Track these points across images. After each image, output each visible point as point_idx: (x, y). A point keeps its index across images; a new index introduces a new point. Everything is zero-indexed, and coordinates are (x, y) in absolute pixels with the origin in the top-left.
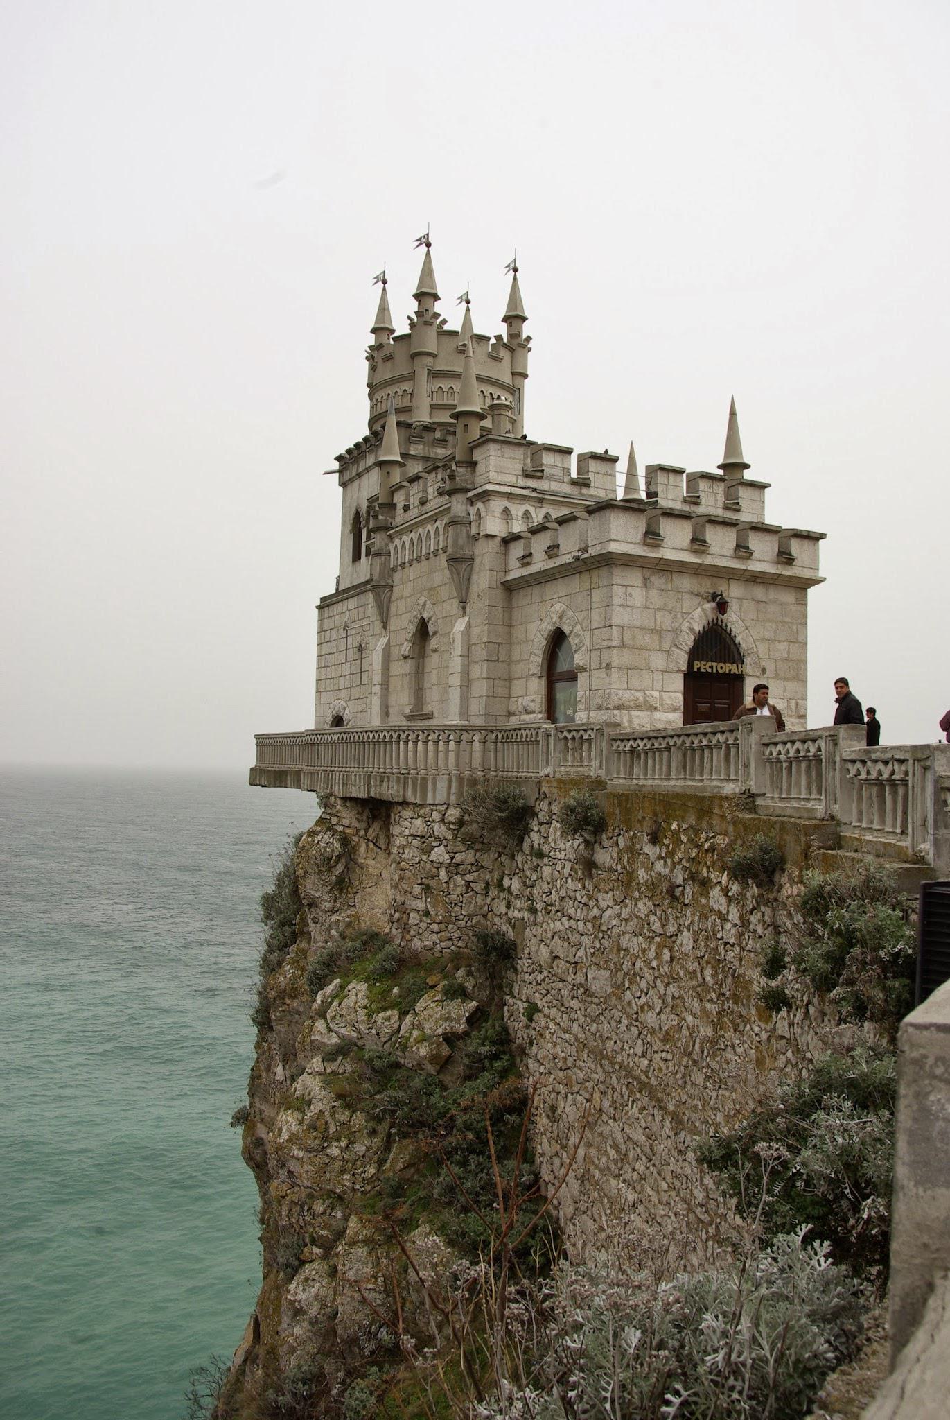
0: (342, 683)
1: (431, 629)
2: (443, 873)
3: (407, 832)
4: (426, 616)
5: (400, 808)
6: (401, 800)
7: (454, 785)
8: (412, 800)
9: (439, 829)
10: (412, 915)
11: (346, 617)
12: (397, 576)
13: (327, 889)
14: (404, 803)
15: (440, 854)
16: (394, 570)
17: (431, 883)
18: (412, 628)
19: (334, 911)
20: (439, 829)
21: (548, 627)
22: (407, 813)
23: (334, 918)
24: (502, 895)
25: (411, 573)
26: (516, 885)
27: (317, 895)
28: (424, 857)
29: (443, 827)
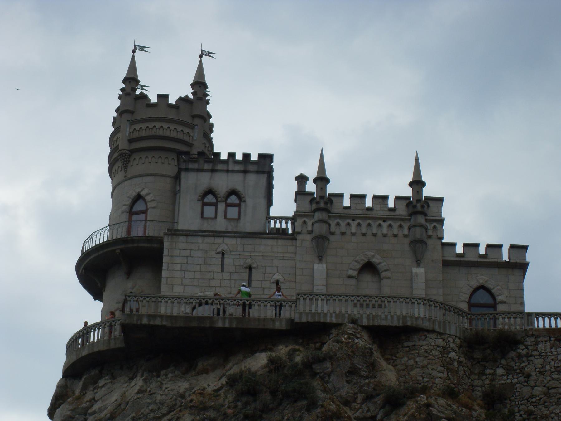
0: (213, 283)
1: (381, 267)
2: (456, 364)
3: (433, 344)
4: (374, 260)
5: (426, 333)
6: (431, 329)
7: (458, 329)
8: (438, 330)
9: (452, 345)
10: (437, 380)
11: (223, 247)
12: (332, 238)
13: (365, 366)
14: (433, 331)
15: (452, 355)
16: (333, 234)
17: (450, 367)
18: (358, 266)
19: (367, 377)
20: (452, 345)
21: (475, 283)
22: (433, 336)
23: (367, 381)
24: (484, 377)
25: (354, 239)
26: (500, 371)
27: (360, 367)
28: (445, 356)
29: (454, 345)
